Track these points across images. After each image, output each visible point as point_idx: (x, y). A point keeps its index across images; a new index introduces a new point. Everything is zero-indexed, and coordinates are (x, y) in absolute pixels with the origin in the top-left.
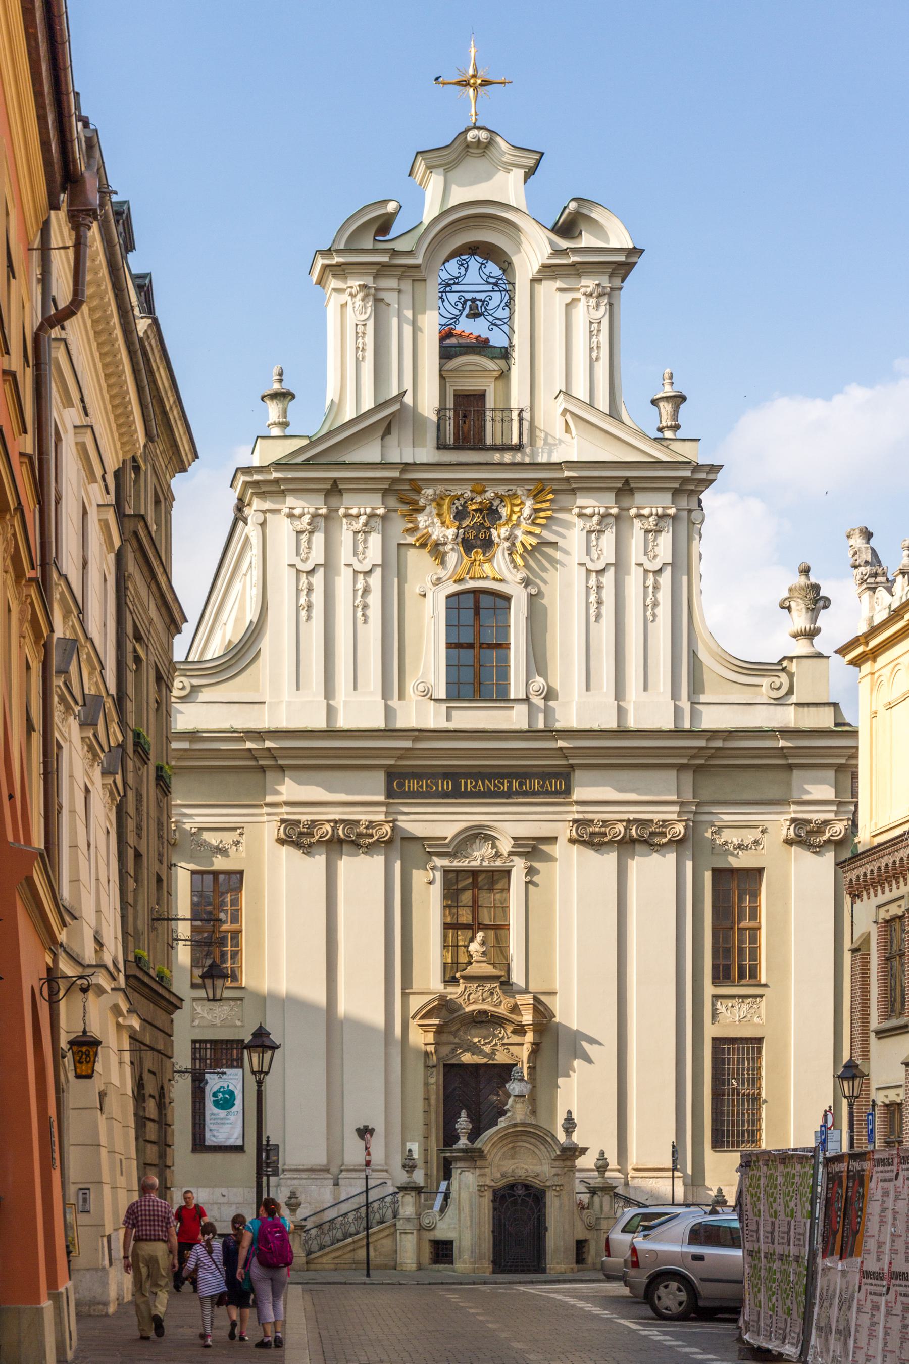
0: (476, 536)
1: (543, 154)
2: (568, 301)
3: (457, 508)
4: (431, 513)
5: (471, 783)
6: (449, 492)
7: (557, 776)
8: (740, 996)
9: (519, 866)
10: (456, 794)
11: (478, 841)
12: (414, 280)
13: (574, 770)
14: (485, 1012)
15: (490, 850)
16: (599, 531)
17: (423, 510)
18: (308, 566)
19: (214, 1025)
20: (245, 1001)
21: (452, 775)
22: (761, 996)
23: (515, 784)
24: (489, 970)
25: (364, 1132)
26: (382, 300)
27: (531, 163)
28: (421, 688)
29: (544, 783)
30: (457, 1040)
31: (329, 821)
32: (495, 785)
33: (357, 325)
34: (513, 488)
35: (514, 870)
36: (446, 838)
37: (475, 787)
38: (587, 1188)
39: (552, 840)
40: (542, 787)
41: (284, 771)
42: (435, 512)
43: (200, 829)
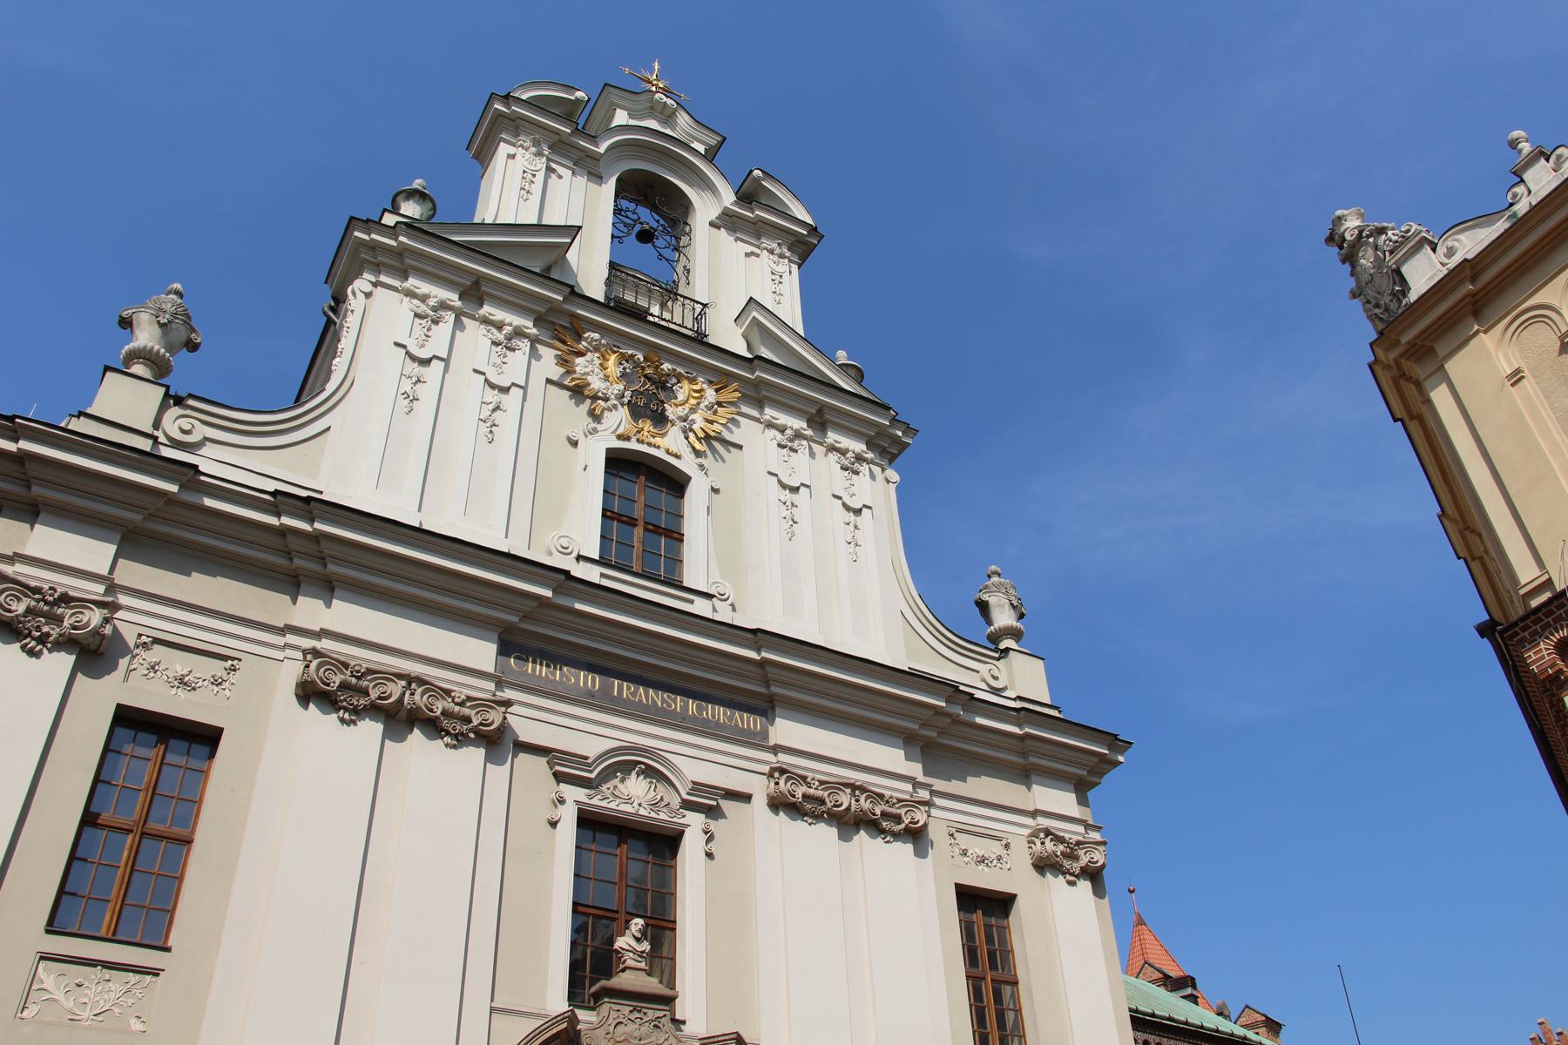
0: (647, 405)
1: (725, 139)
2: (749, 251)
3: (624, 369)
4: (592, 361)
5: (628, 688)
6: (615, 349)
11: (634, 774)
15: (652, 794)
18: (424, 354)
26: (554, 171)
27: (713, 142)
28: (564, 542)
31: (400, 676)
32: (663, 701)
33: (524, 172)
35: (688, 831)
36: (586, 758)
39: (746, 798)
40: (730, 719)
41: (332, 590)
42: (597, 362)
43: (157, 641)
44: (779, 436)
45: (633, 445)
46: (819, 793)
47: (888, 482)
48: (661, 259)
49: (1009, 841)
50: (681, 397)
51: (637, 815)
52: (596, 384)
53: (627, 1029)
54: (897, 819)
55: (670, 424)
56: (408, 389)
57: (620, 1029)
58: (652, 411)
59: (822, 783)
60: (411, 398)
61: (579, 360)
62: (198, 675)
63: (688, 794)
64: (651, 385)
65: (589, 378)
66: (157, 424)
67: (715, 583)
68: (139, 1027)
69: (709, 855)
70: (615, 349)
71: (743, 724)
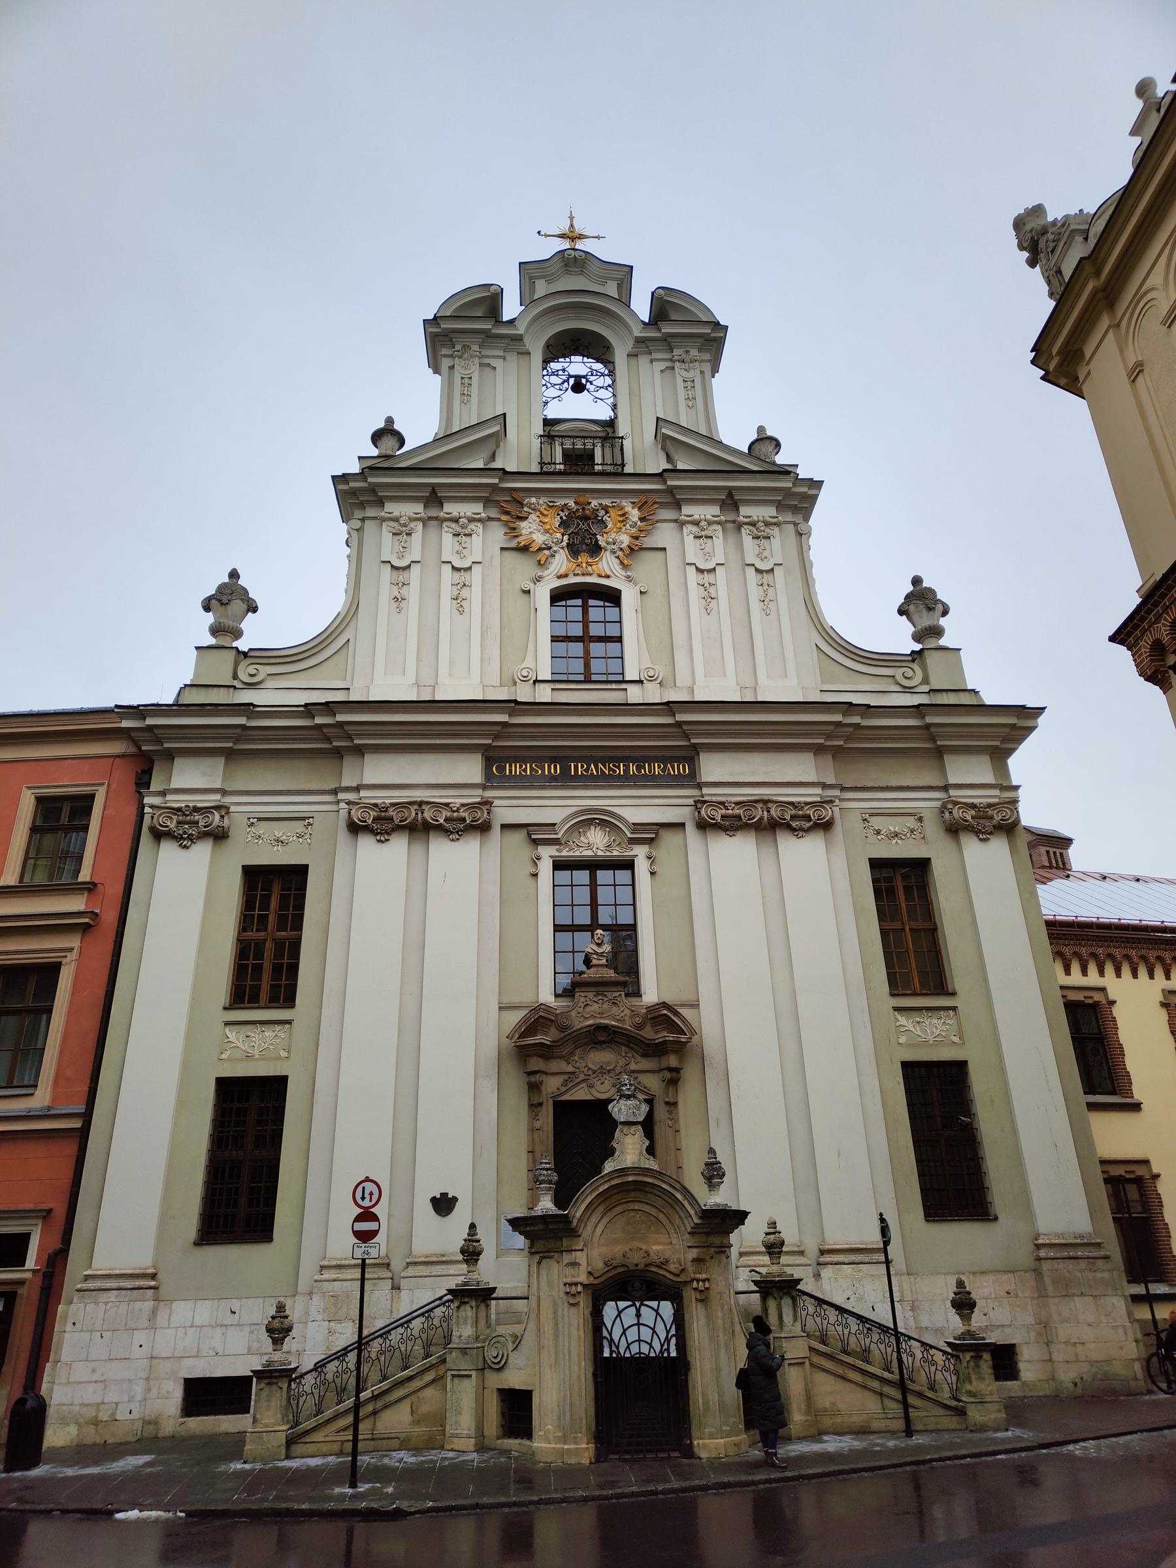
3: (561, 518)
7: (679, 760)
8: (928, 1009)
9: (640, 853)
10: (565, 780)
11: (592, 828)
12: (518, 353)
13: (698, 754)
14: (605, 1028)
16: (706, 537)
17: (527, 518)
19: (249, 1057)
20: (294, 1024)
21: (561, 757)
22: (954, 1009)
23: (633, 769)
24: (610, 974)
25: (443, 1205)
29: (665, 767)
30: (570, 1069)
32: (610, 769)
33: (462, 378)
34: (618, 501)
37: (587, 770)
38: (756, 1283)
43: (259, 819)
44: (694, 529)
45: (573, 580)
46: (737, 812)
47: (801, 535)
48: (596, 402)
49: (922, 815)
50: (610, 525)
51: (596, 856)
52: (539, 538)
53: (592, 1008)
54: (807, 818)
55: (603, 550)
56: (396, 594)
57: (588, 1009)
58: (587, 545)
59: (737, 803)
60: (400, 599)
61: (523, 524)
62: (289, 834)
63: (632, 833)
64: (583, 524)
65: (534, 537)
66: (235, 677)
67: (646, 669)
68: (286, 1054)
69: (652, 874)
70: (551, 504)
71: (674, 772)
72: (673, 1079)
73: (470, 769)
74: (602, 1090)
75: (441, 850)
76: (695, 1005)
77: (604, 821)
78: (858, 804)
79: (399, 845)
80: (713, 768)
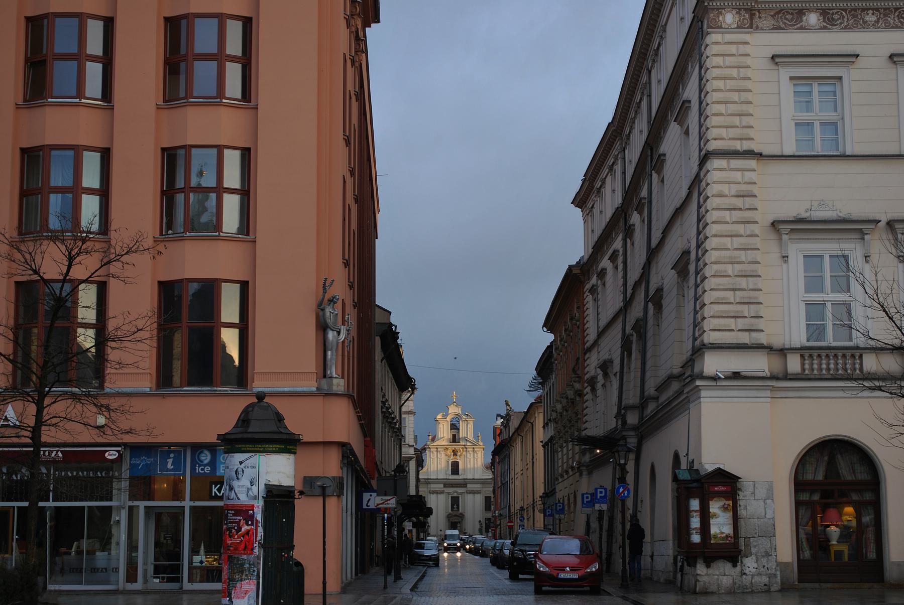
9: (460, 496)
10: (452, 487)
21: (452, 484)
25: (441, 530)
72: (462, 520)
73: (442, 486)
74: (456, 521)
75: (439, 495)
76: (465, 513)
77: (456, 492)
78: (484, 489)
79: (435, 495)
80: (468, 486)
